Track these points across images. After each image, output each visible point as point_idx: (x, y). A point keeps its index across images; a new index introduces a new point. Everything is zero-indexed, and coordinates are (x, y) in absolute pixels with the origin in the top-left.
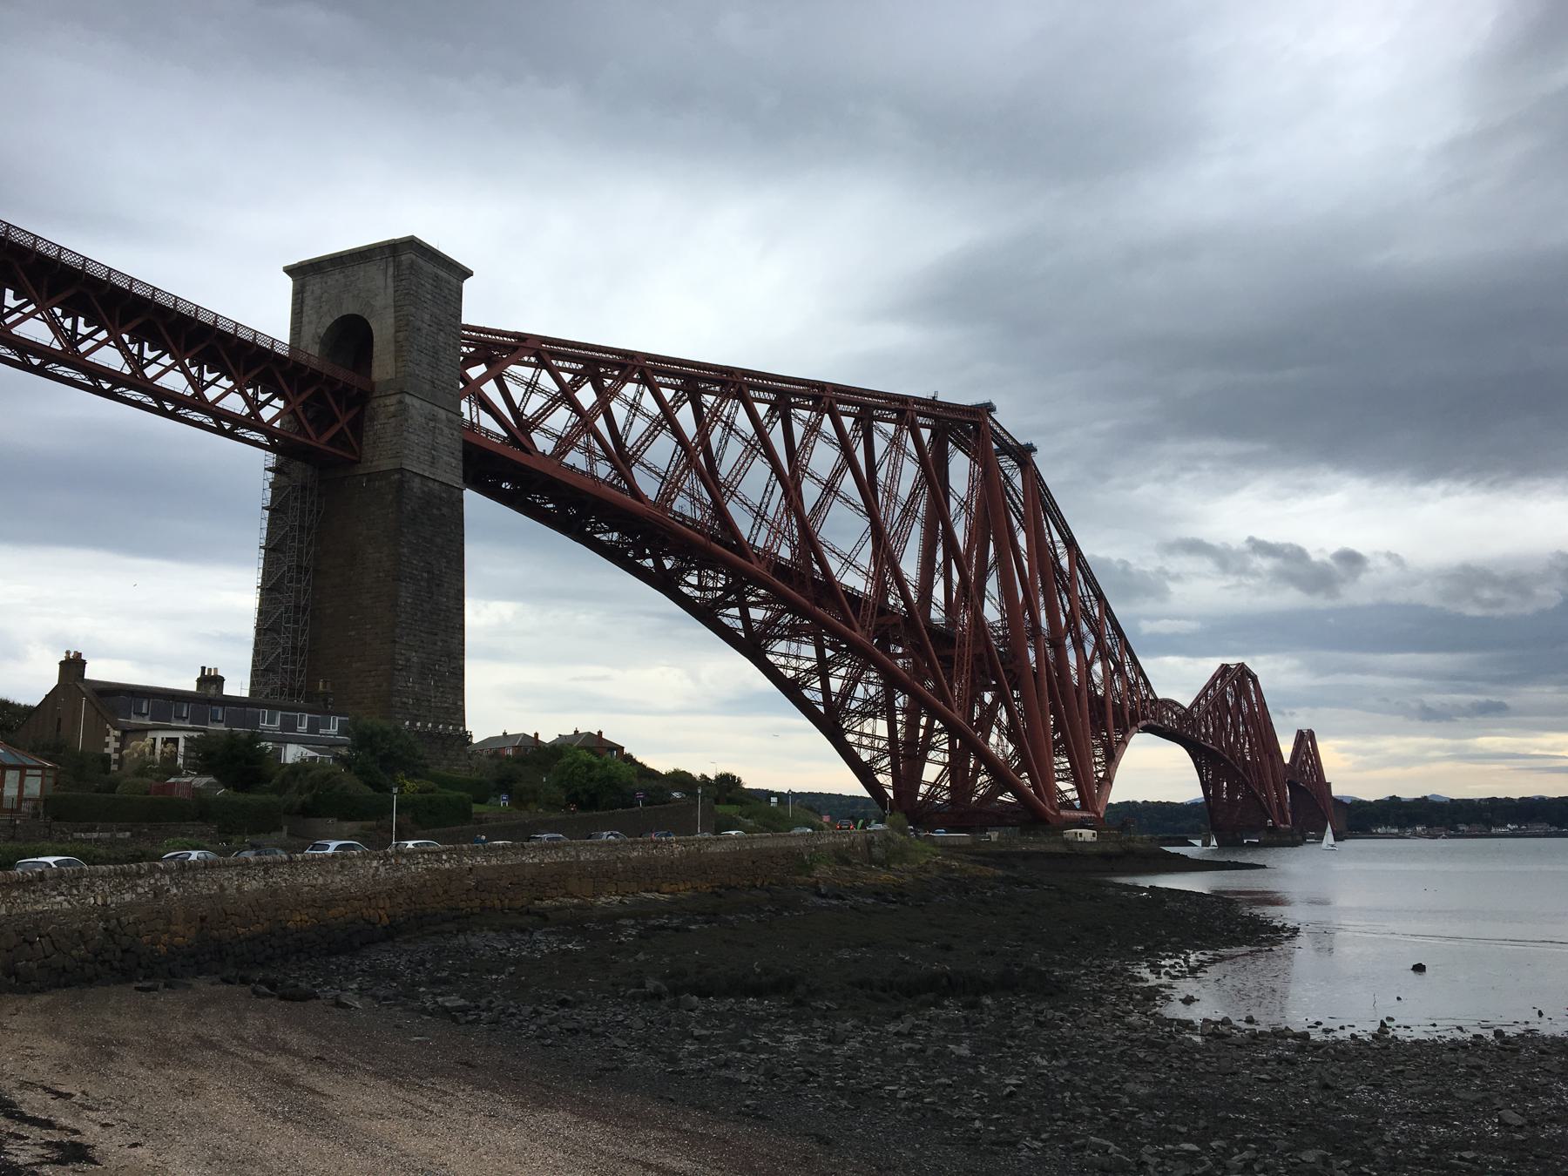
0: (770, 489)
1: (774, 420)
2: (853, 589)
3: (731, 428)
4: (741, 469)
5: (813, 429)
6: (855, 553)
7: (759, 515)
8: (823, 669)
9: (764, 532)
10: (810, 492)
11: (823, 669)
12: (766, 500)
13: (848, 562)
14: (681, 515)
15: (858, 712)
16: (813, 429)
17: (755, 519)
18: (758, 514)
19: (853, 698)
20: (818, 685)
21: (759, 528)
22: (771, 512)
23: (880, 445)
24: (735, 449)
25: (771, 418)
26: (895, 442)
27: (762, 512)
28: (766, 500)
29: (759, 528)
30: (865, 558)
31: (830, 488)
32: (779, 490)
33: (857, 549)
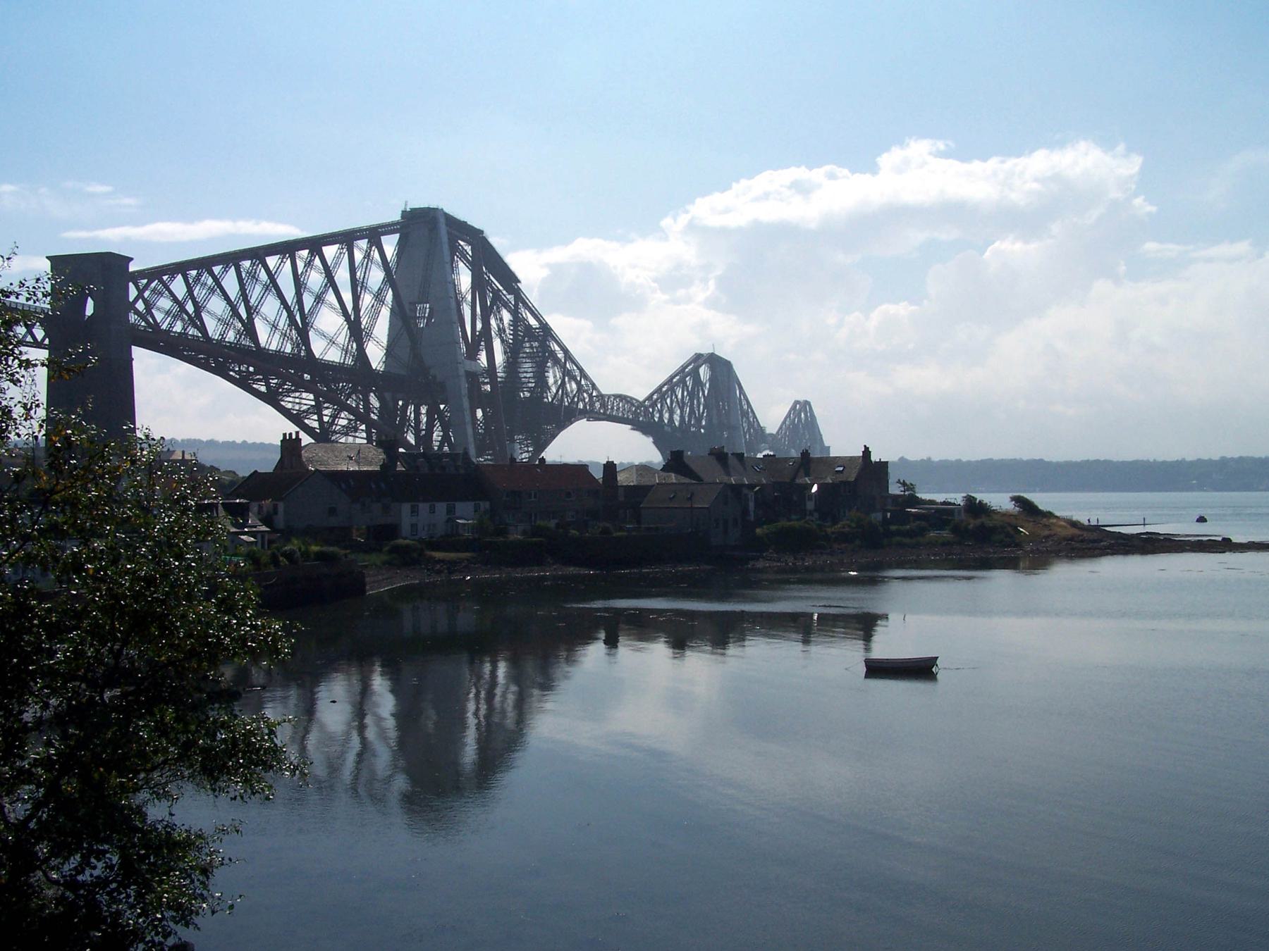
0: (280, 313)
1: (285, 260)
2: (333, 362)
3: (257, 280)
4: (261, 300)
5: (309, 264)
6: (336, 336)
7: (274, 326)
8: (318, 409)
9: (277, 336)
10: (308, 301)
11: (318, 409)
12: (278, 318)
13: (332, 342)
14: (229, 342)
15: (339, 433)
16: (309, 264)
17: (272, 329)
18: (273, 326)
19: (336, 425)
20: (315, 417)
21: (274, 334)
22: (281, 325)
23: (358, 256)
24: (258, 289)
25: (283, 259)
26: (367, 256)
27: (276, 324)
28: (278, 318)
29: (274, 334)
30: (343, 338)
31: (319, 299)
32: (285, 314)
33: (338, 334)
